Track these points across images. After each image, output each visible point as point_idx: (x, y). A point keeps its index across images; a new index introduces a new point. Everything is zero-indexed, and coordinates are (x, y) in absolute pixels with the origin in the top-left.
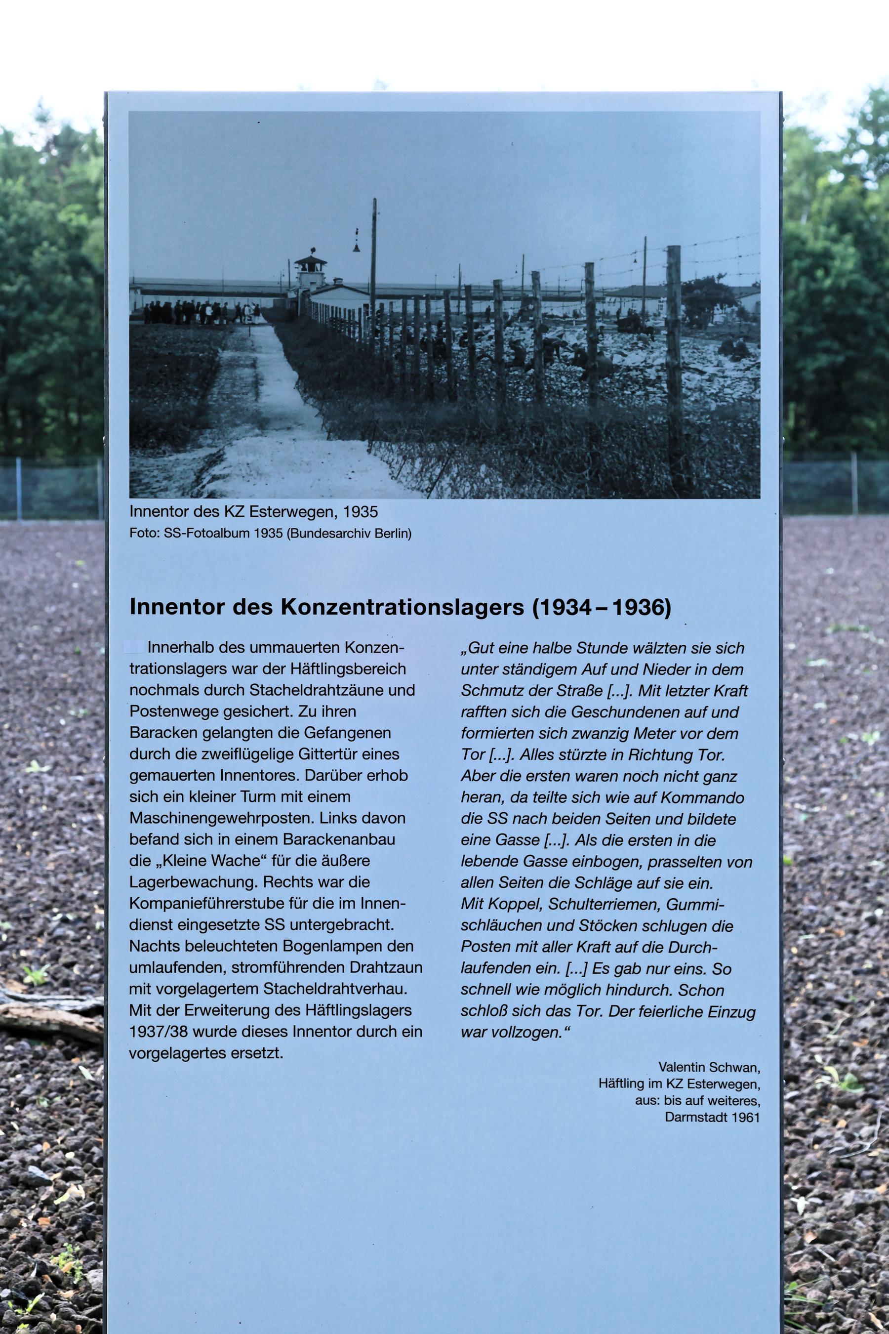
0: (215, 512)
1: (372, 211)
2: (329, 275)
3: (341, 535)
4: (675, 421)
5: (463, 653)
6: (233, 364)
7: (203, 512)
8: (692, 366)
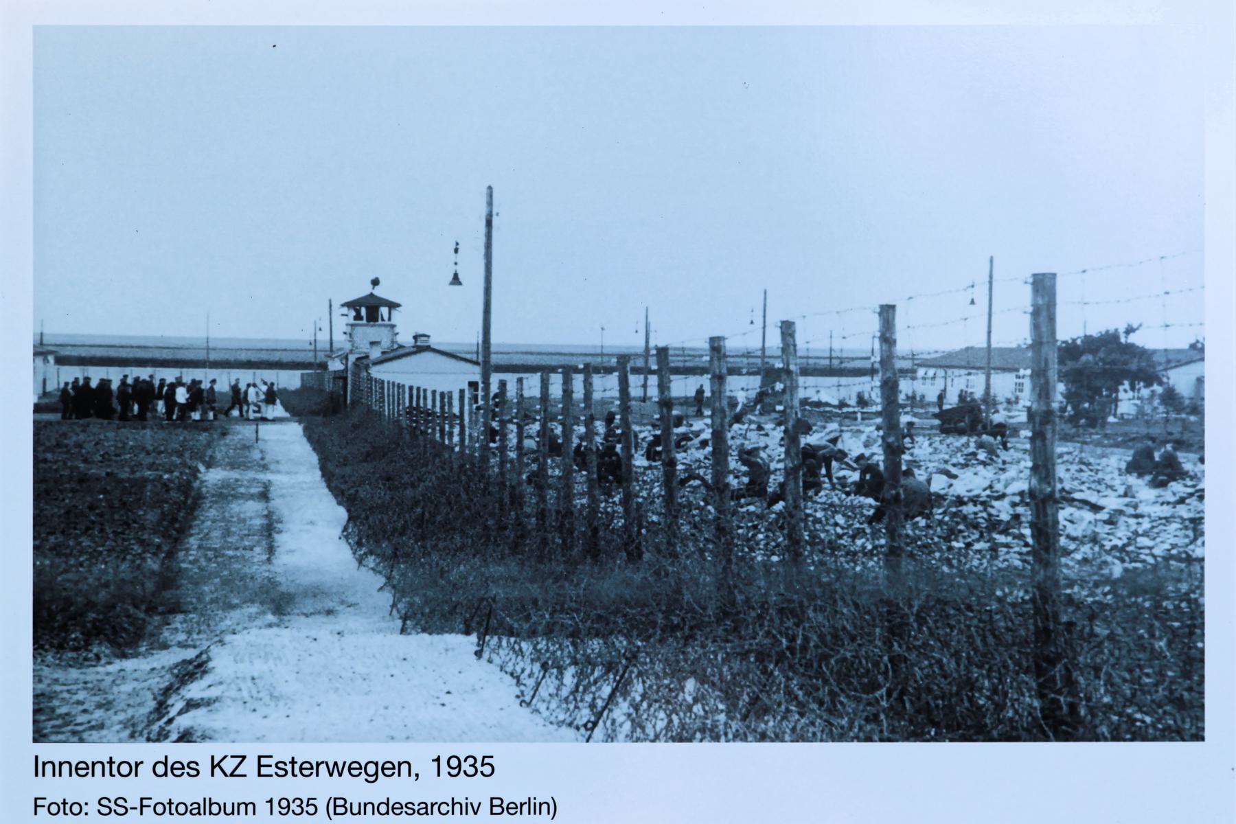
0: (192, 768)
1: (483, 211)
2: (405, 328)
3: (426, 809)
4: (1045, 598)
6: (226, 494)
7: (170, 768)
8: (1077, 496)
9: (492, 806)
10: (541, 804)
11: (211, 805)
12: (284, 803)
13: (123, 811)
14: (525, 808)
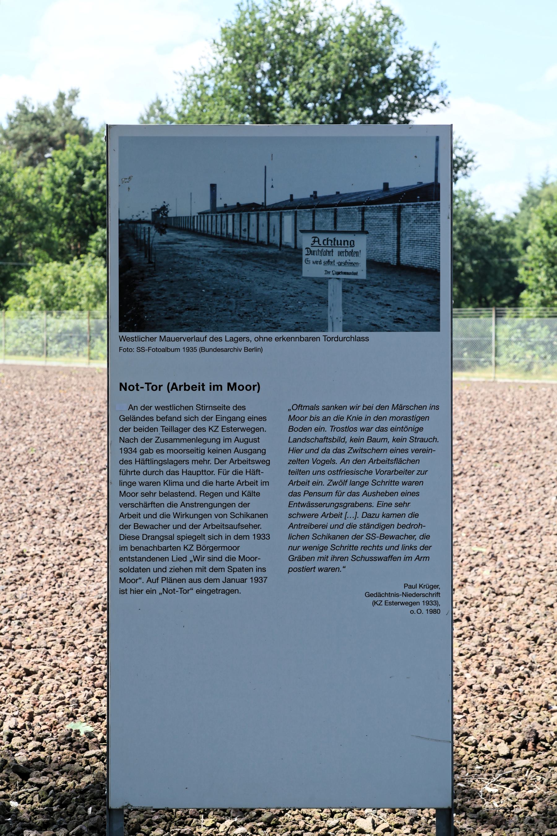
3: (227, 350)
5: (289, 410)
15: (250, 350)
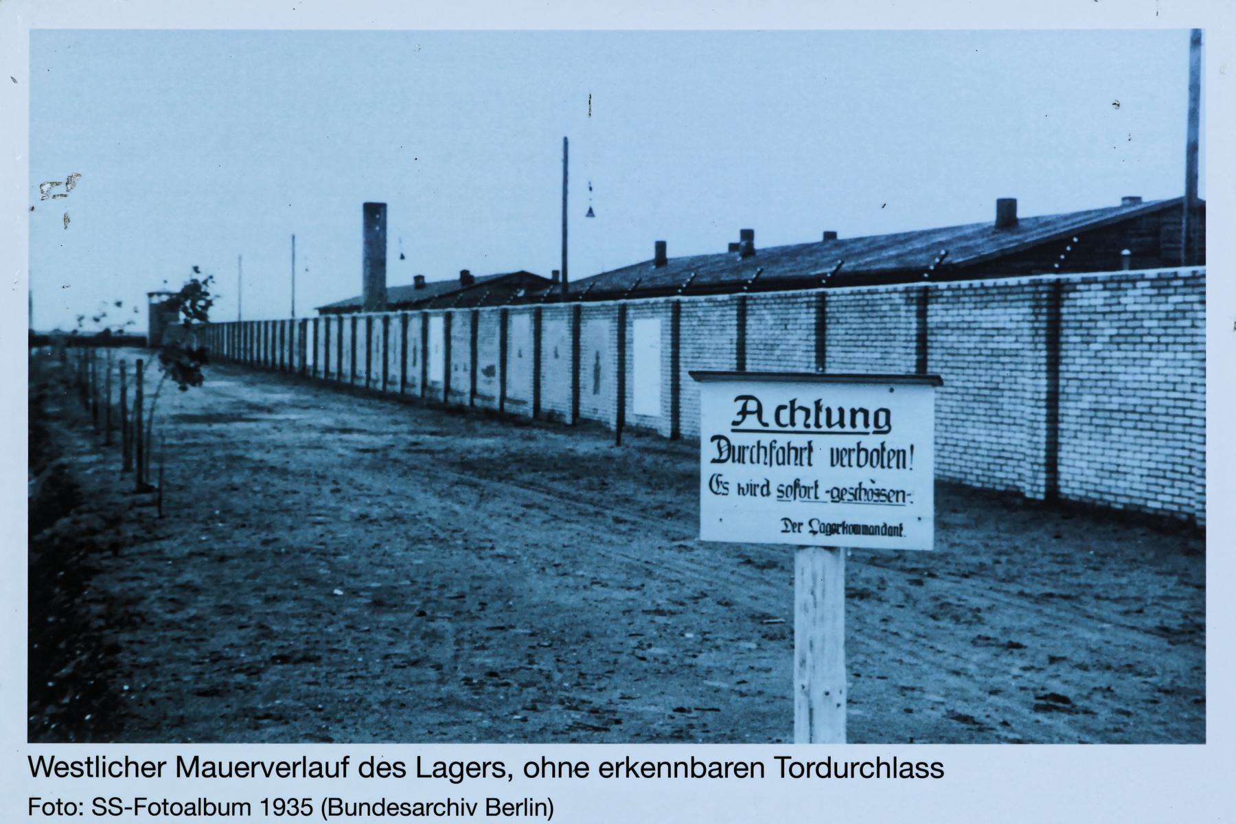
3: (422, 810)
9: (488, 807)
10: (537, 805)
11: (206, 805)
12: (279, 804)
13: (117, 811)
14: (522, 808)
15: (509, 809)
